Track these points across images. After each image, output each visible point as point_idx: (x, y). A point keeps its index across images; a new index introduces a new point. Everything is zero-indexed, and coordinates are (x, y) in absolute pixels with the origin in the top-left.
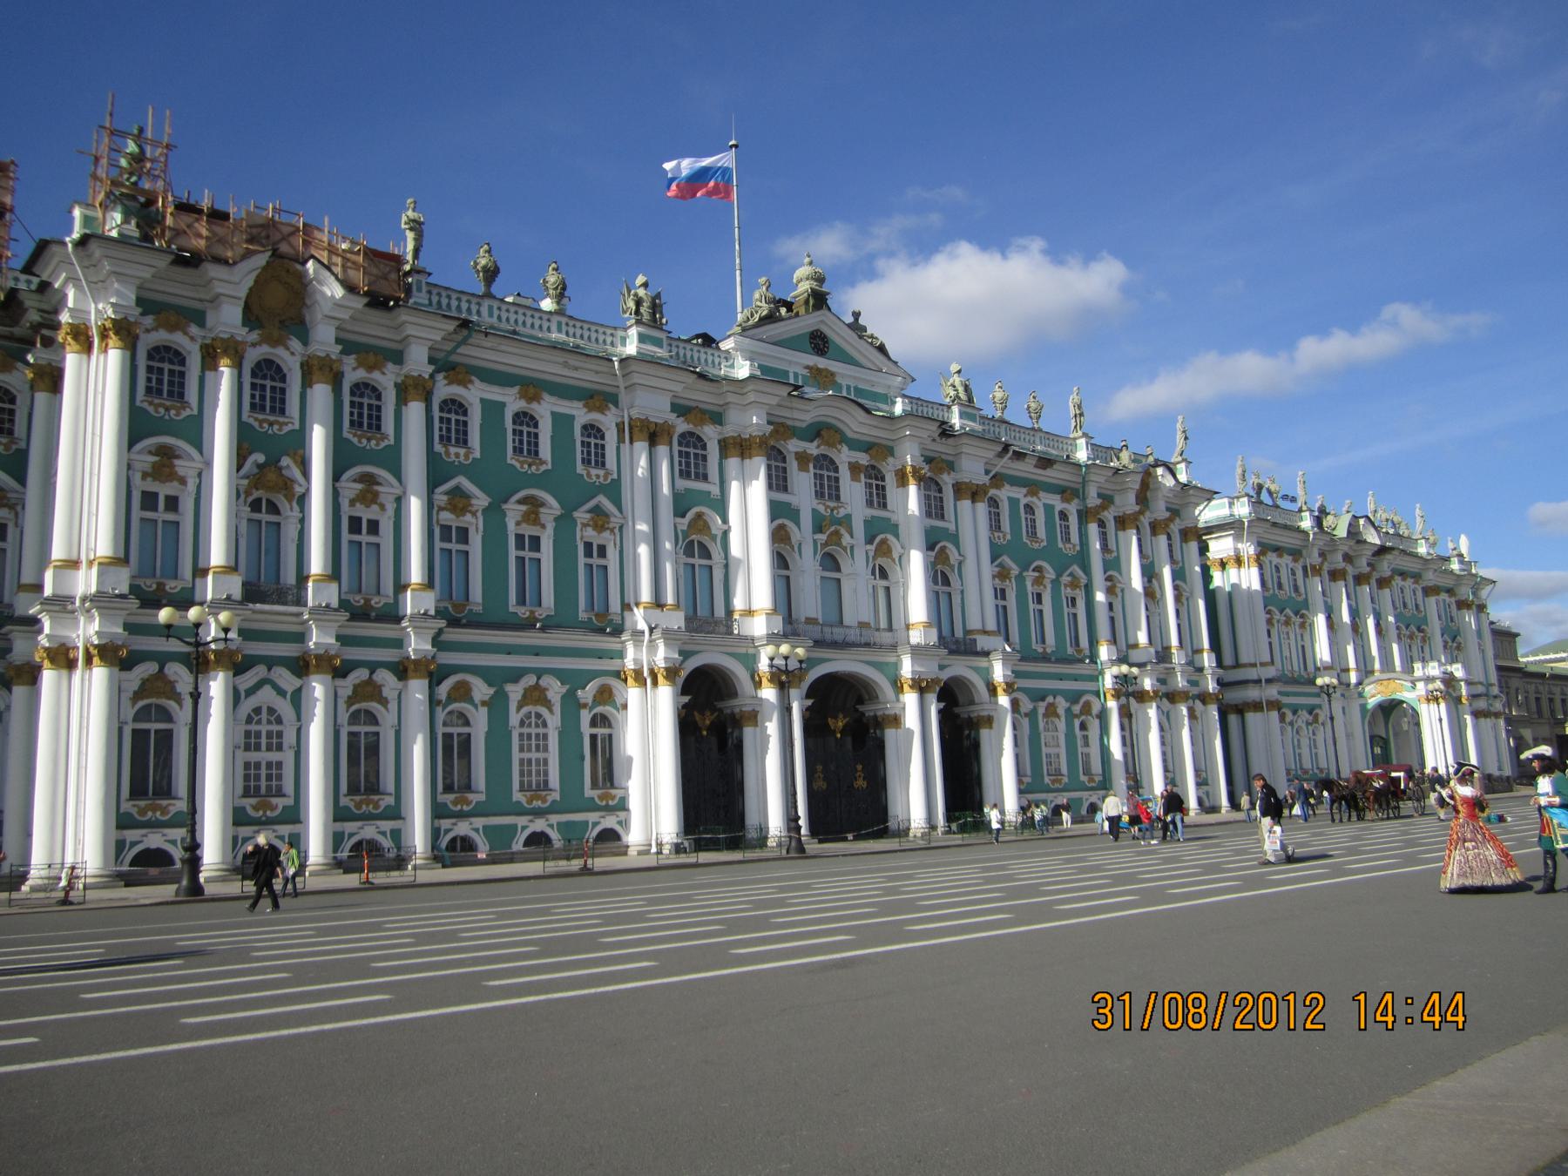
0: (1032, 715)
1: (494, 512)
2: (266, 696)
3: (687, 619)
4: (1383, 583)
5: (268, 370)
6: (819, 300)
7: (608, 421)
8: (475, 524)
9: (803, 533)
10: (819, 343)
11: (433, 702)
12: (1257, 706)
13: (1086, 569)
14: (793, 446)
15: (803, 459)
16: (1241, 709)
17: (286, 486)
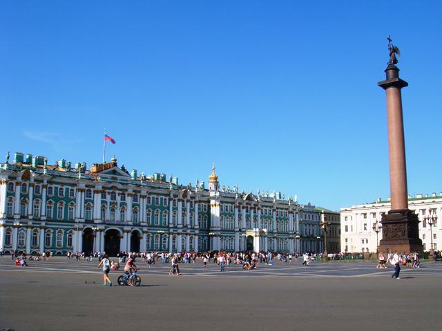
0: (152, 237)
1: (55, 205)
2: (22, 231)
3: (86, 220)
4: (258, 209)
5: (25, 185)
6: (115, 165)
7: (75, 188)
8: (53, 206)
9: (108, 207)
10: (114, 172)
11: (45, 232)
12: (215, 236)
13: (169, 210)
14: (107, 191)
15: (109, 193)
16: (212, 236)
17: (26, 202)
